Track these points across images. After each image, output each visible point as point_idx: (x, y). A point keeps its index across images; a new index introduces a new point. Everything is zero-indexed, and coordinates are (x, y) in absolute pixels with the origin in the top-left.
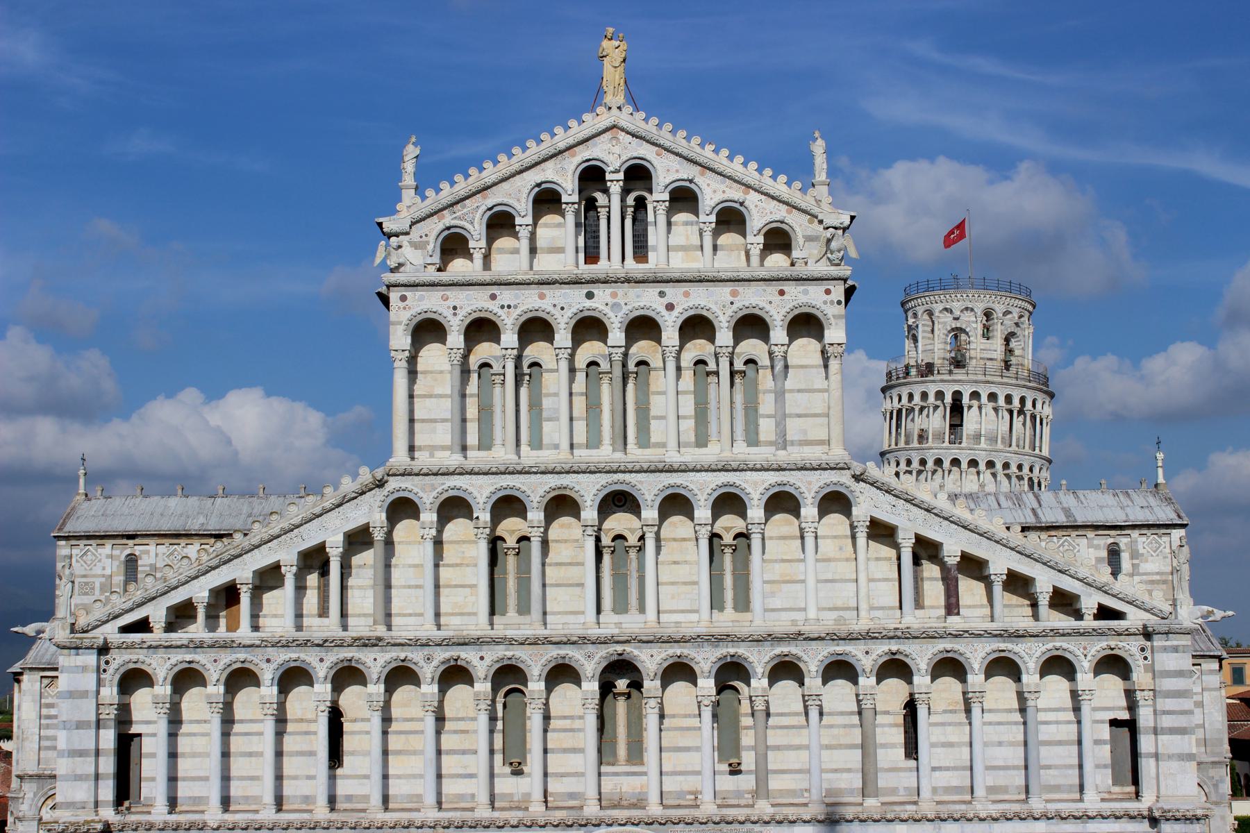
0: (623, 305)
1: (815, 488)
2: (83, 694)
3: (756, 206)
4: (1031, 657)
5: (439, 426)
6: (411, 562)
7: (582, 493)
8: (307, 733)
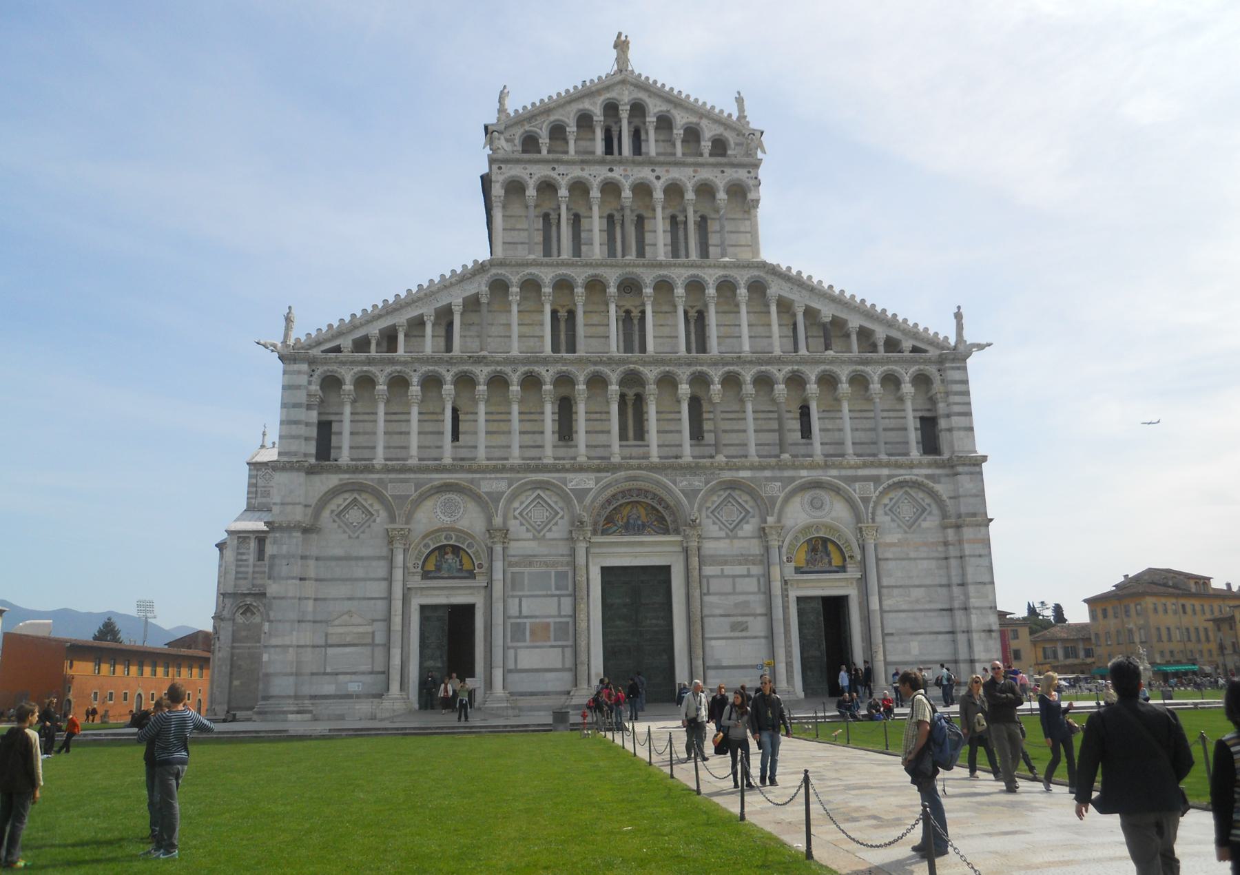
1: (746, 278)
2: (298, 387)
4: (875, 373)
5: (520, 246)
6: (502, 322)
7: (608, 278)
8: (437, 421)
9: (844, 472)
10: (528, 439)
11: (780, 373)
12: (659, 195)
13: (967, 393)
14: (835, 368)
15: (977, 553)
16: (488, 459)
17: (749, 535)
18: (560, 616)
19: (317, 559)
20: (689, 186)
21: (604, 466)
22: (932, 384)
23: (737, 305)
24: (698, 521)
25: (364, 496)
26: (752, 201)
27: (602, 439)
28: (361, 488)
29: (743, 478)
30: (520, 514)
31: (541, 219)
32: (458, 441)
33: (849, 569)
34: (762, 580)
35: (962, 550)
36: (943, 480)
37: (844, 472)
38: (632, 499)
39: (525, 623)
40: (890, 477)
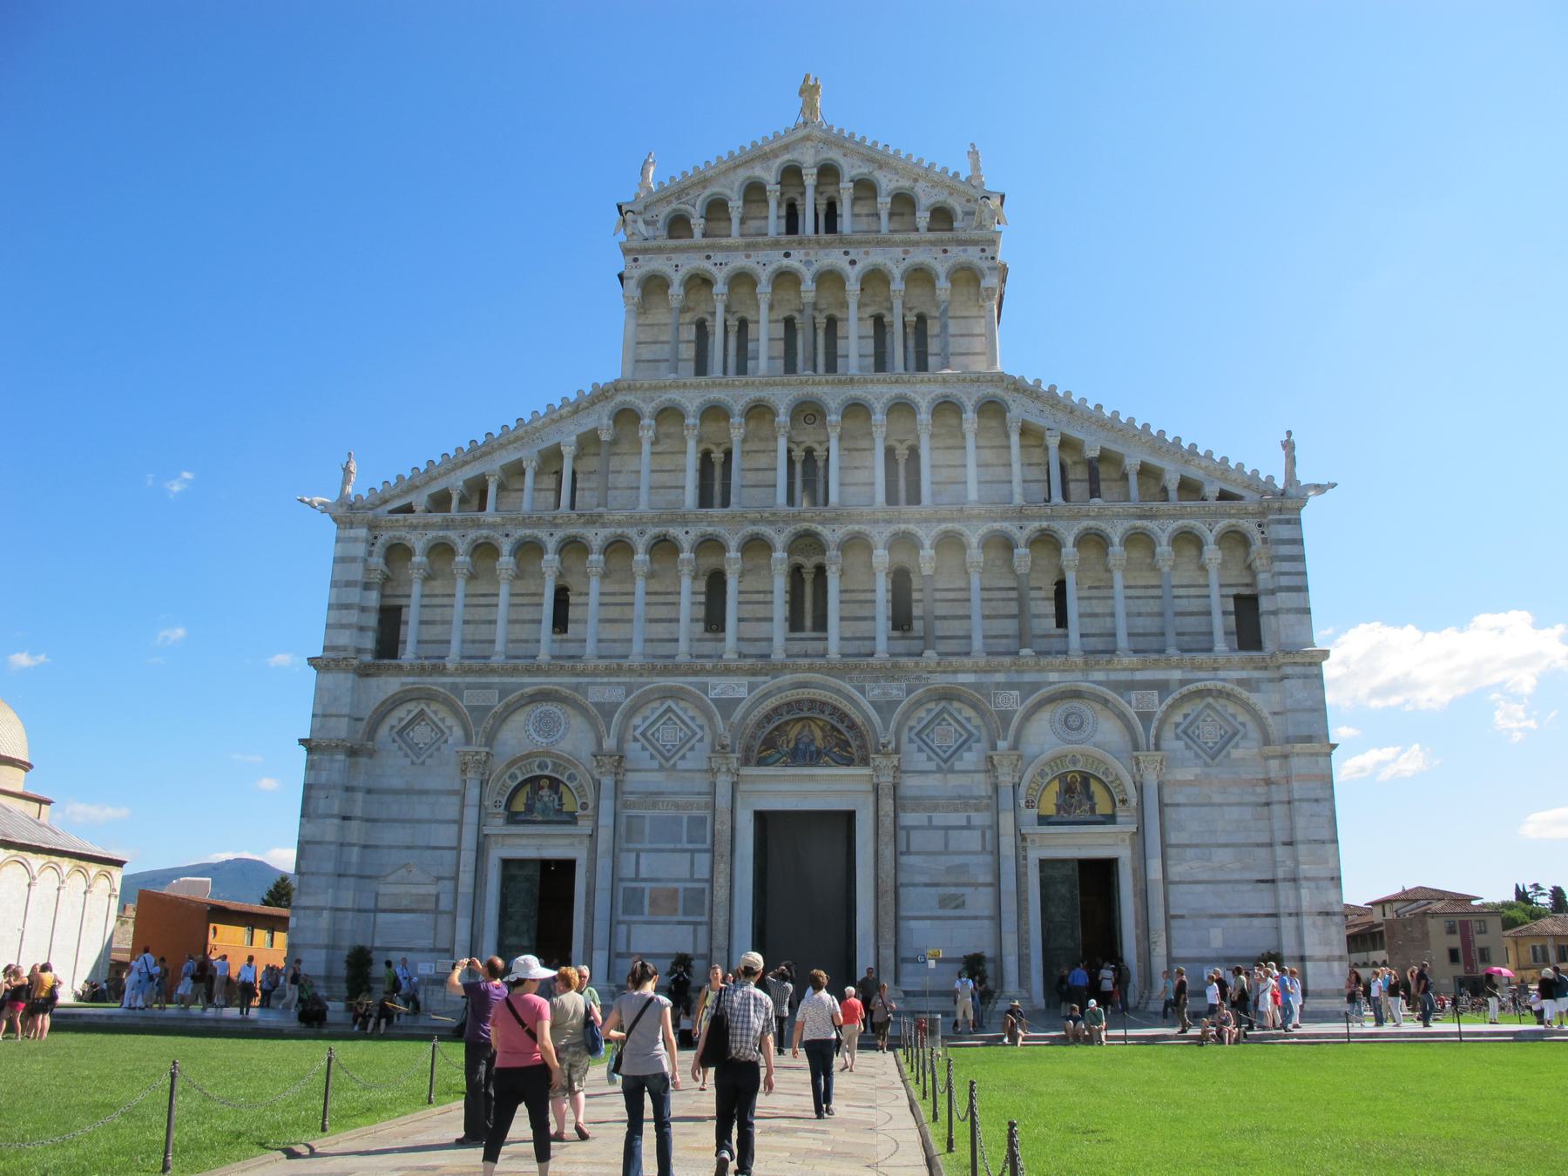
1: (975, 398)
2: (353, 560)
4: (1163, 531)
5: (663, 366)
6: (634, 468)
10: (660, 630)
12: (853, 287)
13: (1301, 558)
14: (1102, 525)
15: (1313, 795)
16: (601, 657)
17: (973, 768)
18: (692, 880)
19: (369, 791)
20: (897, 272)
21: (762, 664)
22: (1250, 546)
23: (964, 437)
24: (890, 747)
25: (434, 706)
27: (761, 630)
28: (429, 696)
29: (963, 684)
30: (643, 734)
31: (694, 327)
32: (566, 632)
33: (1119, 819)
34: (988, 834)
35: (1290, 791)
36: (1264, 686)
37: (1114, 676)
38: (802, 715)
39: (643, 889)
40: (1183, 683)
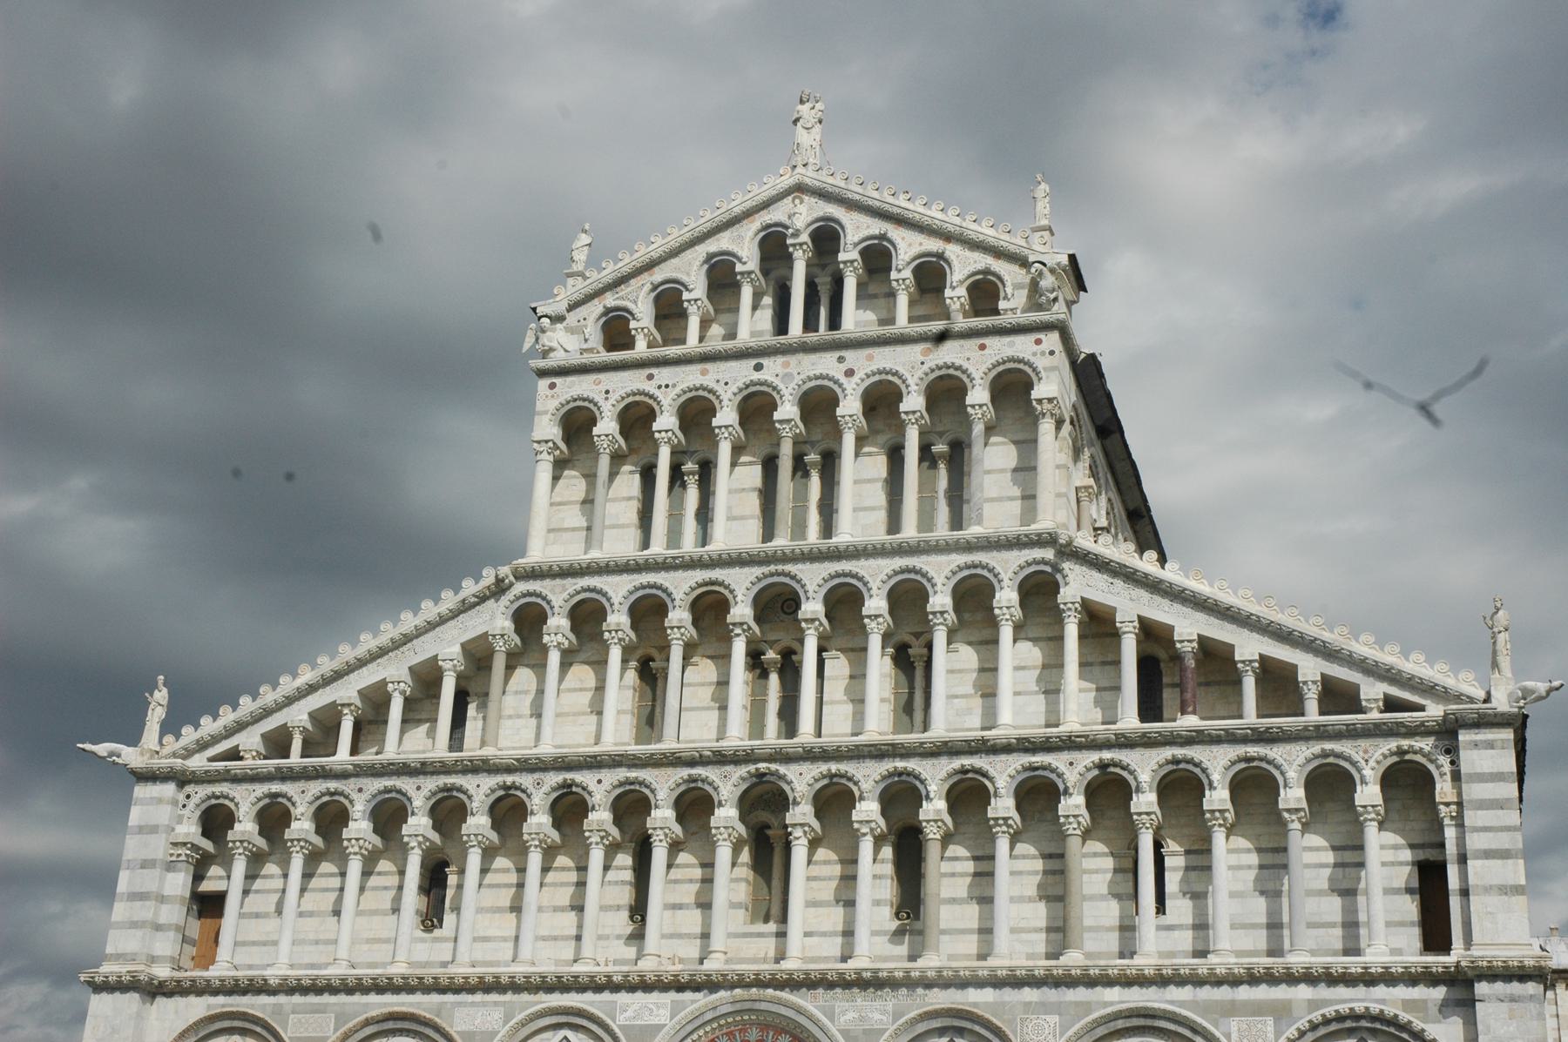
0: (796, 374)
1: (1015, 567)
2: (153, 829)
3: (958, 256)
9: (1207, 993)
11: (1074, 770)
26: (1040, 401)
29: (975, 1005)
40: (1314, 1005)
